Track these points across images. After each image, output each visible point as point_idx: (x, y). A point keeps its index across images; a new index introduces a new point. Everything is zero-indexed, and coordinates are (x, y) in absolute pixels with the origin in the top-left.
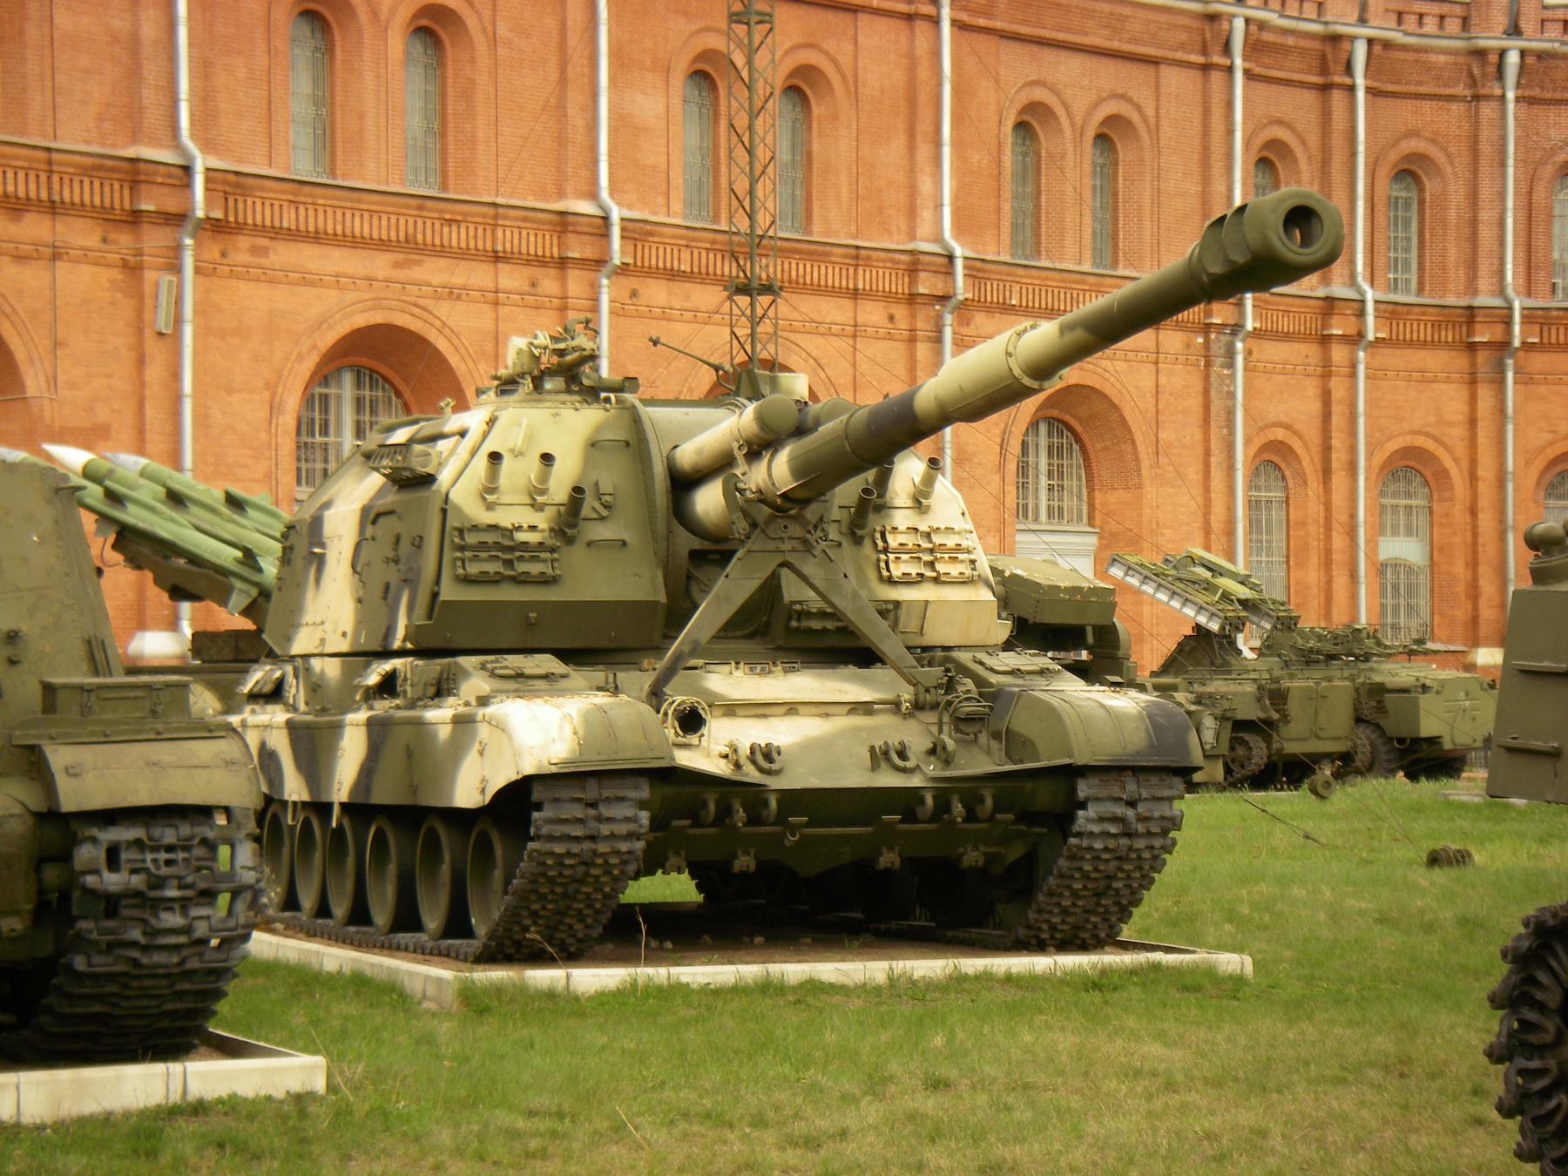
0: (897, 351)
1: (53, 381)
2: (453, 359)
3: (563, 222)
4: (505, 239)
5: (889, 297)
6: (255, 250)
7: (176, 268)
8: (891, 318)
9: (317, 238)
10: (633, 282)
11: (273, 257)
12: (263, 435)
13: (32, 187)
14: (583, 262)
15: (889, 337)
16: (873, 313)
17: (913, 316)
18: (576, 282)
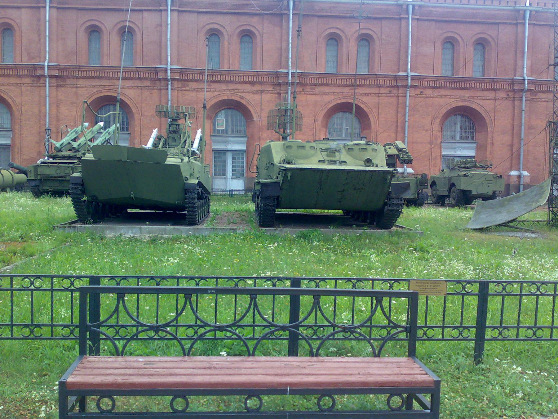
0: (509, 103)
1: (260, 117)
2: (365, 109)
3: (396, 78)
4: (380, 82)
5: (505, 90)
6: (311, 89)
7: (287, 93)
8: (508, 95)
9: (328, 85)
10: (422, 90)
11: (316, 89)
12: (312, 126)
13: (255, 79)
14: (402, 86)
15: (506, 99)
16: (502, 95)
17: (515, 94)
18: (401, 91)
